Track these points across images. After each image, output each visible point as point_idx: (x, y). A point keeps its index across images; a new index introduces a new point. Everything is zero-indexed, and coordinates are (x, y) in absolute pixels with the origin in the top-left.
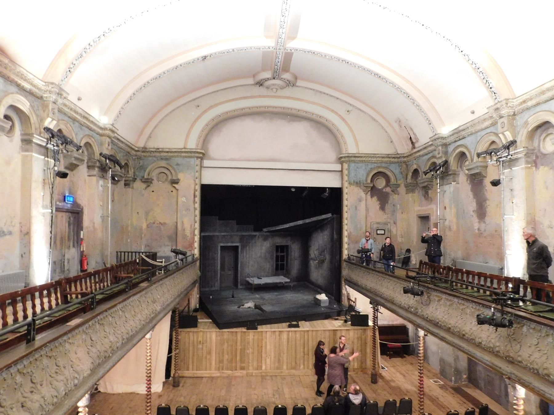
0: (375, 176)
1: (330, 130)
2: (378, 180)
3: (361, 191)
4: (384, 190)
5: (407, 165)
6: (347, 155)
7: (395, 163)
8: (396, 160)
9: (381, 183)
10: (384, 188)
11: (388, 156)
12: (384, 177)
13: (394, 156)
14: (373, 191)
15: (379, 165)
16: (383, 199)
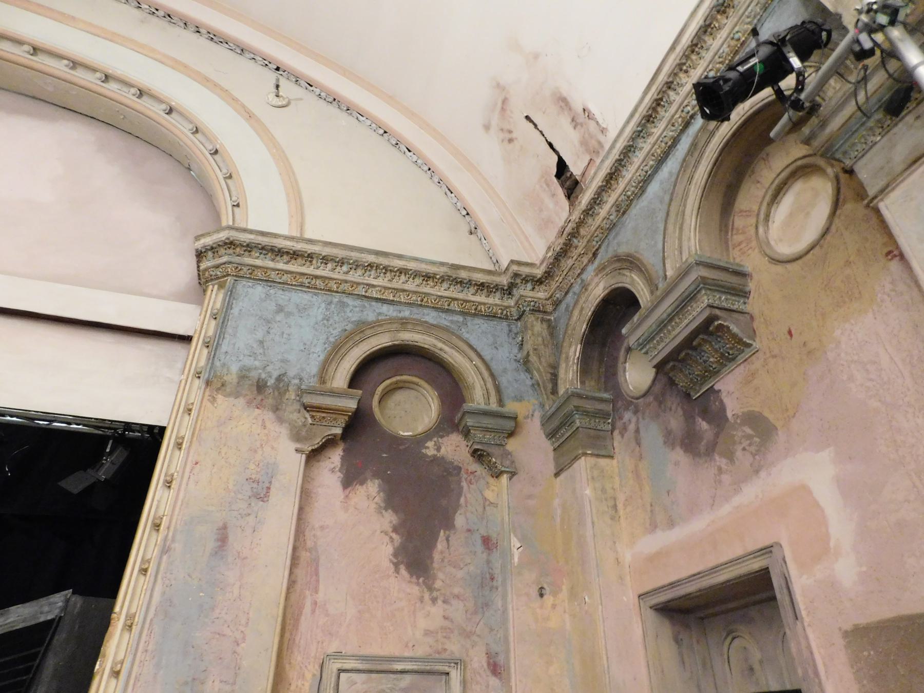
0: (377, 371)
1: (184, 165)
2: (399, 396)
3: (283, 432)
4: (430, 449)
5: (552, 328)
6: (223, 236)
7: (492, 316)
8: (495, 300)
9: (411, 411)
10: (428, 435)
11: (453, 277)
12: (432, 382)
13: (480, 278)
14: (355, 436)
15: (406, 313)
16: (422, 507)
